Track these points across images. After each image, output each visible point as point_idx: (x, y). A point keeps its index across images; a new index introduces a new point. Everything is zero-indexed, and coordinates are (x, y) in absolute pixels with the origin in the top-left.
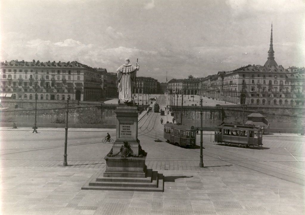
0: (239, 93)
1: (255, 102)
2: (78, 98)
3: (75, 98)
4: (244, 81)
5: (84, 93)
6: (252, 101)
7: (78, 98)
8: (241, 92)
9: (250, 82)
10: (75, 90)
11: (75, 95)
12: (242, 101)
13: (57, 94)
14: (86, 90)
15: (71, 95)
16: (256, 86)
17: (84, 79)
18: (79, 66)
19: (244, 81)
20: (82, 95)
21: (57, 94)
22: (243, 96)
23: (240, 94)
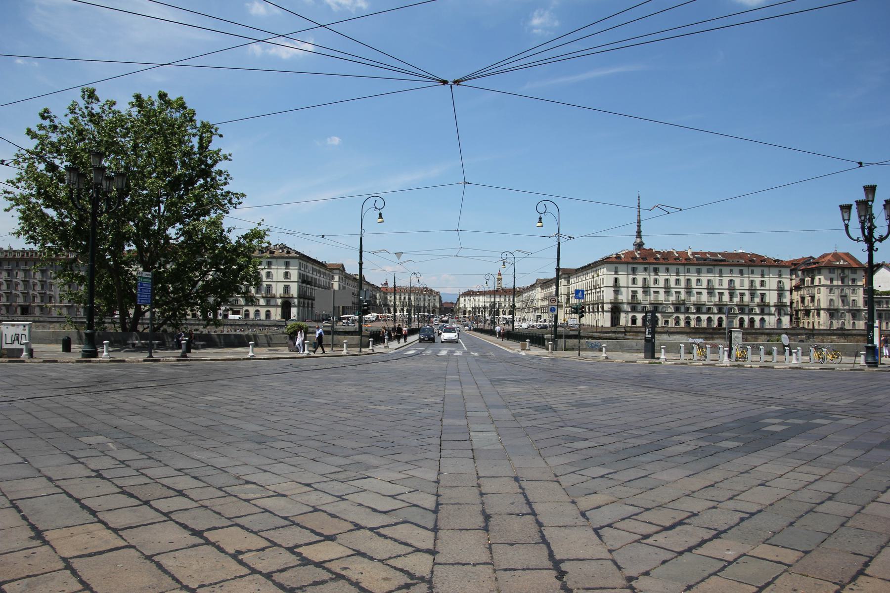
0: (607, 303)
1: (639, 322)
2: (286, 314)
3: (278, 318)
4: (616, 280)
5: (299, 306)
6: (634, 321)
7: (286, 314)
8: (611, 303)
9: (628, 282)
10: (279, 301)
11: (279, 310)
12: (615, 321)
13: (245, 308)
14: (302, 300)
15: (272, 310)
16: (640, 291)
17: (299, 278)
18: (288, 252)
19: (616, 280)
20: (294, 311)
21: (245, 308)
22: (616, 310)
23: (610, 306)
